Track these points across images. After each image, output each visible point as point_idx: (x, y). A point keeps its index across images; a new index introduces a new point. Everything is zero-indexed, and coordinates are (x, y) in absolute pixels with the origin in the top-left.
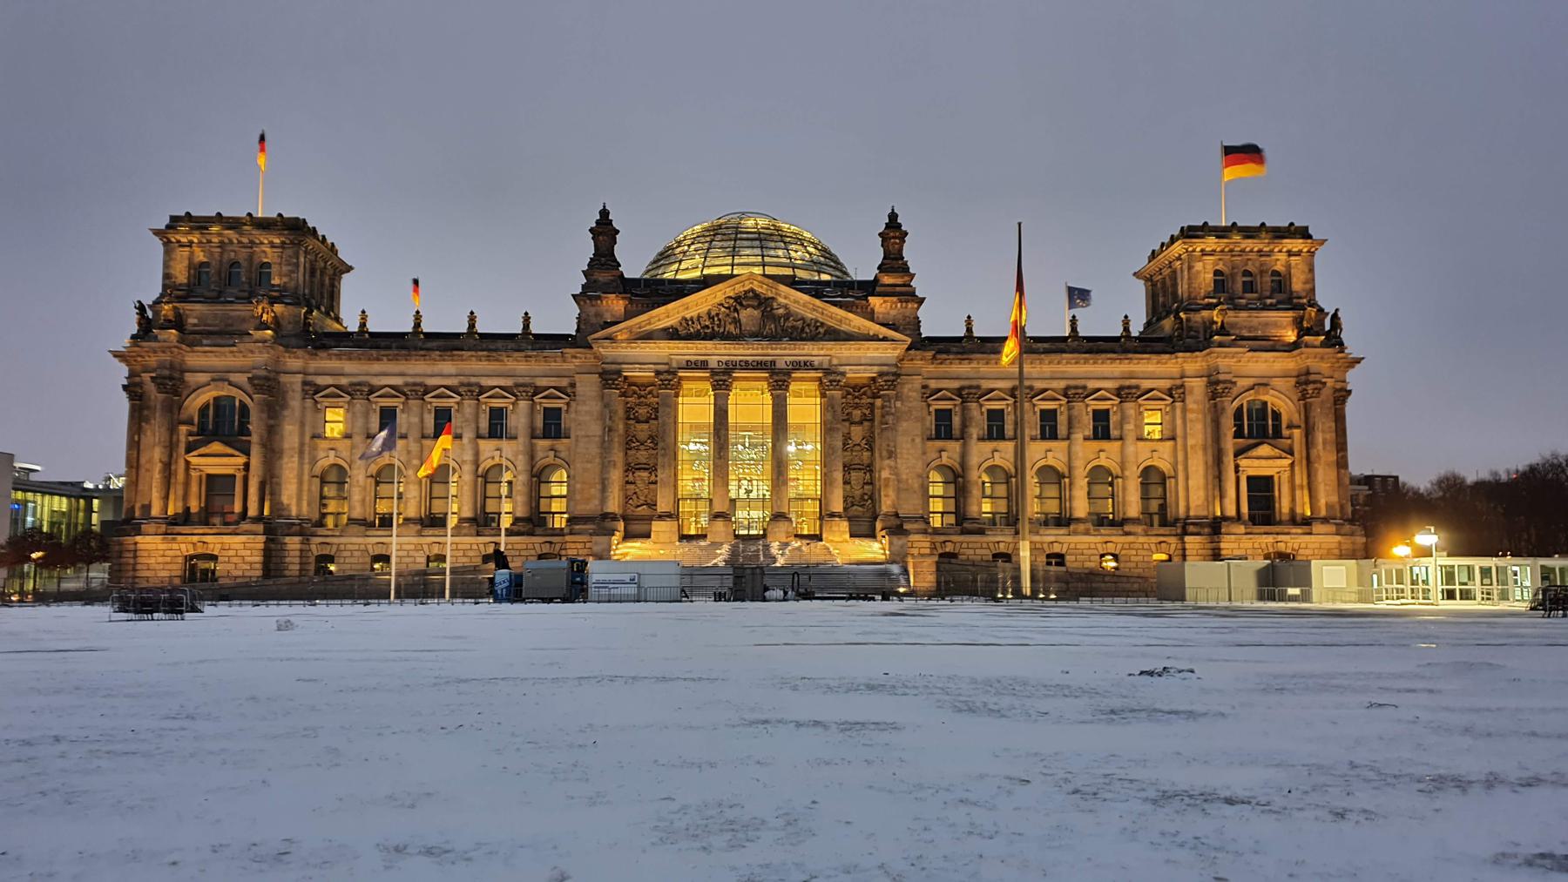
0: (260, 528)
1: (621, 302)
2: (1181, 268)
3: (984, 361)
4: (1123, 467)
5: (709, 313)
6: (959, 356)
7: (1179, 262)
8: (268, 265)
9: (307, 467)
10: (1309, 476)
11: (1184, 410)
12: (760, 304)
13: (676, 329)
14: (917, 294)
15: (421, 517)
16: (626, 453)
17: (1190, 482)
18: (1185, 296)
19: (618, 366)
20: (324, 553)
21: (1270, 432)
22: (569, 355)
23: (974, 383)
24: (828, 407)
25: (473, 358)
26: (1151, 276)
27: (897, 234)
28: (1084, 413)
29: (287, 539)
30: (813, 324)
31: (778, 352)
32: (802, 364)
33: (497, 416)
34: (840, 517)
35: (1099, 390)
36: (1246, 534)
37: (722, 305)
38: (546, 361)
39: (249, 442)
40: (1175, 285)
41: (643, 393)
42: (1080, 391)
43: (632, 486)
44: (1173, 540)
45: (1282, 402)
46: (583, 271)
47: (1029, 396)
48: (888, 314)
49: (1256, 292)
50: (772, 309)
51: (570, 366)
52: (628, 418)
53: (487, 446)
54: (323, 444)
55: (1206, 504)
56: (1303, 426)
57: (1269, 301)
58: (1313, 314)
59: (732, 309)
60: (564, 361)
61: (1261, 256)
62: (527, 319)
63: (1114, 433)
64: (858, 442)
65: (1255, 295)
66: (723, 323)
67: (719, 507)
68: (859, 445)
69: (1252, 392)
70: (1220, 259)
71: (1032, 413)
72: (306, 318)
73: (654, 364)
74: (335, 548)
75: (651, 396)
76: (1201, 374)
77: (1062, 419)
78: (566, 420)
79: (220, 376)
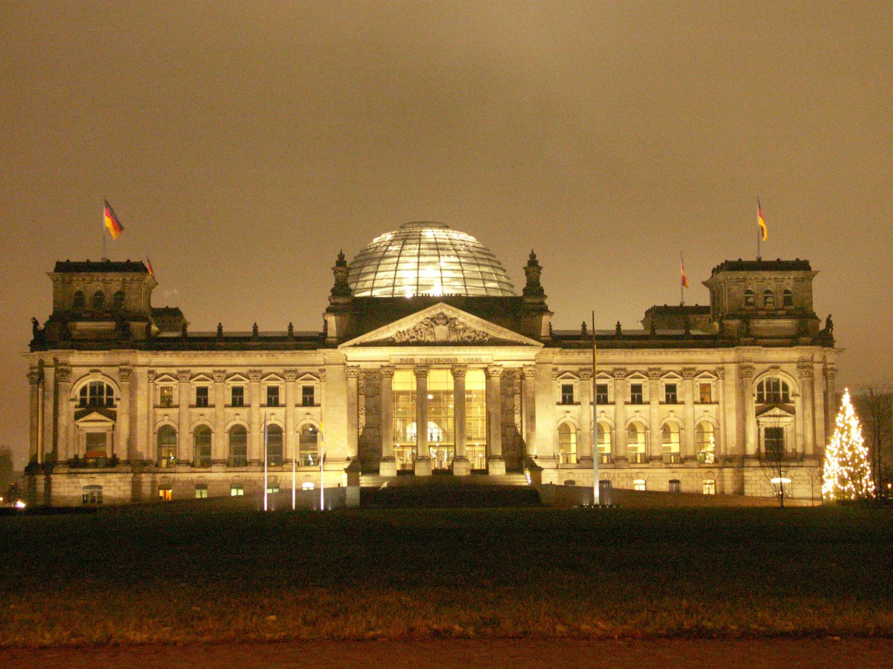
0: (129, 468)
5: (414, 328)
12: (447, 322)
13: (394, 339)
22: (322, 354)
32: (475, 360)
37: (421, 323)
42: (657, 372)
44: (716, 471)
50: (455, 325)
56: (801, 394)
59: (430, 326)
63: (679, 399)
66: (423, 334)
69: (767, 373)
79: (95, 369)
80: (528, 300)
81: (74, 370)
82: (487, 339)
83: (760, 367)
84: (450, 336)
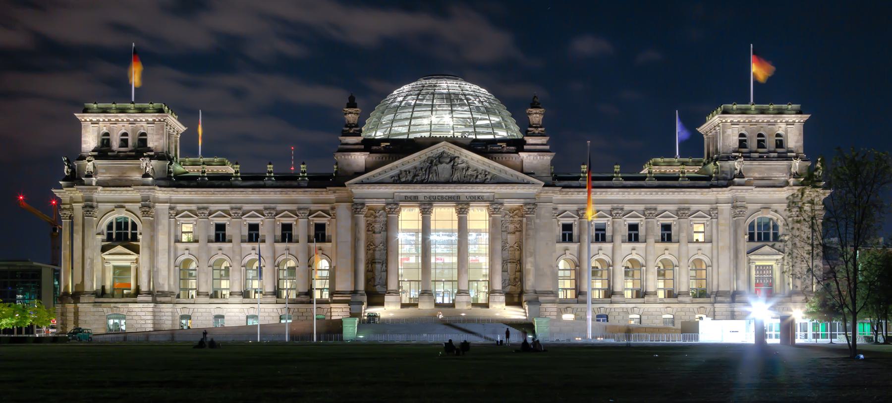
0: (150, 298)
1: (363, 157)
2: (720, 131)
7: (718, 128)
8: (144, 134)
9: (172, 261)
11: (718, 223)
12: (450, 161)
15: (241, 292)
16: (367, 252)
22: (332, 191)
24: (493, 224)
27: (538, 111)
30: (483, 173)
32: (477, 198)
33: (287, 228)
38: (316, 194)
42: (653, 212)
47: (621, 215)
48: (532, 163)
49: (766, 148)
52: (368, 231)
53: (280, 246)
54: (179, 245)
57: (772, 155)
58: (797, 164)
61: (769, 125)
63: (674, 238)
66: (427, 172)
68: (513, 247)
69: (760, 212)
70: (743, 127)
71: (623, 225)
72: (169, 168)
73: (385, 199)
74: (191, 310)
75: (382, 216)
77: (642, 231)
78: (328, 231)
79: (120, 205)
82: (489, 177)
83: (751, 206)
84: (452, 174)
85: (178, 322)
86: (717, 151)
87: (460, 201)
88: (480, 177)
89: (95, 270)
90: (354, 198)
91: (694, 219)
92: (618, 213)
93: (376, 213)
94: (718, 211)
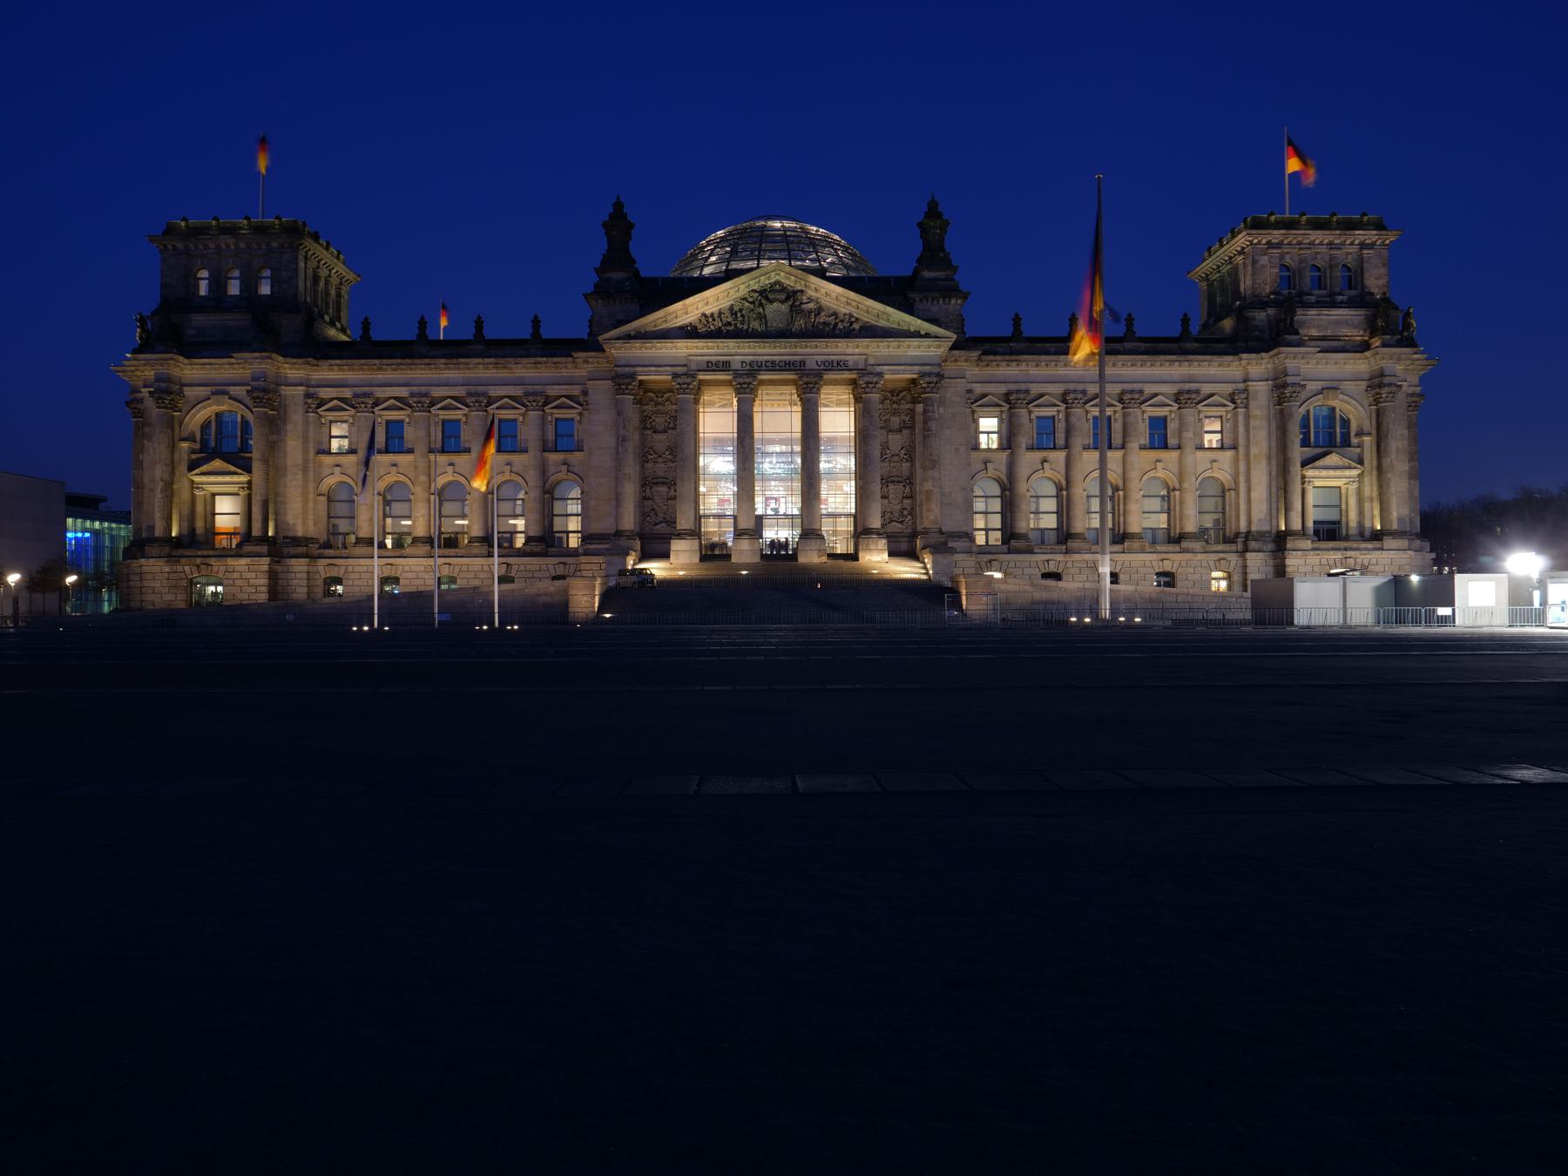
0: (264, 549)
3: (1034, 364)
4: (1181, 476)
5: (731, 308)
6: (1007, 357)
9: (311, 485)
10: (1380, 487)
11: (1247, 417)
13: (696, 327)
14: (960, 289)
15: (431, 537)
17: (1254, 495)
18: (1249, 292)
19: (632, 369)
20: (333, 575)
21: (1338, 440)
22: (581, 360)
23: (1023, 387)
25: (481, 366)
26: (1207, 275)
28: (1140, 420)
29: (293, 561)
31: (808, 350)
32: (835, 364)
34: (879, 534)
35: (1156, 395)
36: (1313, 549)
37: (745, 299)
38: (556, 368)
39: (251, 458)
40: (1236, 282)
41: (660, 399)
42: (1136, 396)
43: (650, 502)
44: (1234, 559)
45: (1354, 409)
46: (595, 268)
47: (1081, 401)
49: (1325, 289)
50: (802, 303)
51: (582, 371)
54: (328, 460)
55: (1268, 518)
56: (1374, 432)
57: (1339, 298)
59: (757, 302)
60: (576, 367)
61: (1331, 249)
62: (536, 323)
63: (1172, 441)
64: (897, 452)
65: (1324, 292)
66: (746, 319)
67: (743, 525)
68: (898, 455)
69: (1321, 395)
74: (343, 569)
76: (1266, 377)
80: (927, 274)
81: (188, 391)
82: (856, 326)
84: (792, 321)
85: (319, 590)
86: (1236, 293)
87: (805, 370)
88: (840, 326)
89: (176, 500)
90: (616, 366)
91: (1205, 409)
92: (1076, 399)
93: (657, 397)
94: (1248, 394)
